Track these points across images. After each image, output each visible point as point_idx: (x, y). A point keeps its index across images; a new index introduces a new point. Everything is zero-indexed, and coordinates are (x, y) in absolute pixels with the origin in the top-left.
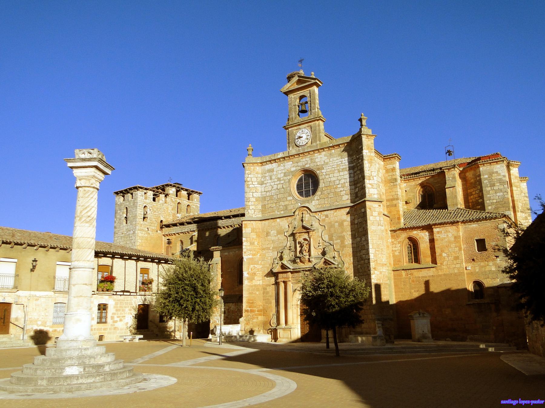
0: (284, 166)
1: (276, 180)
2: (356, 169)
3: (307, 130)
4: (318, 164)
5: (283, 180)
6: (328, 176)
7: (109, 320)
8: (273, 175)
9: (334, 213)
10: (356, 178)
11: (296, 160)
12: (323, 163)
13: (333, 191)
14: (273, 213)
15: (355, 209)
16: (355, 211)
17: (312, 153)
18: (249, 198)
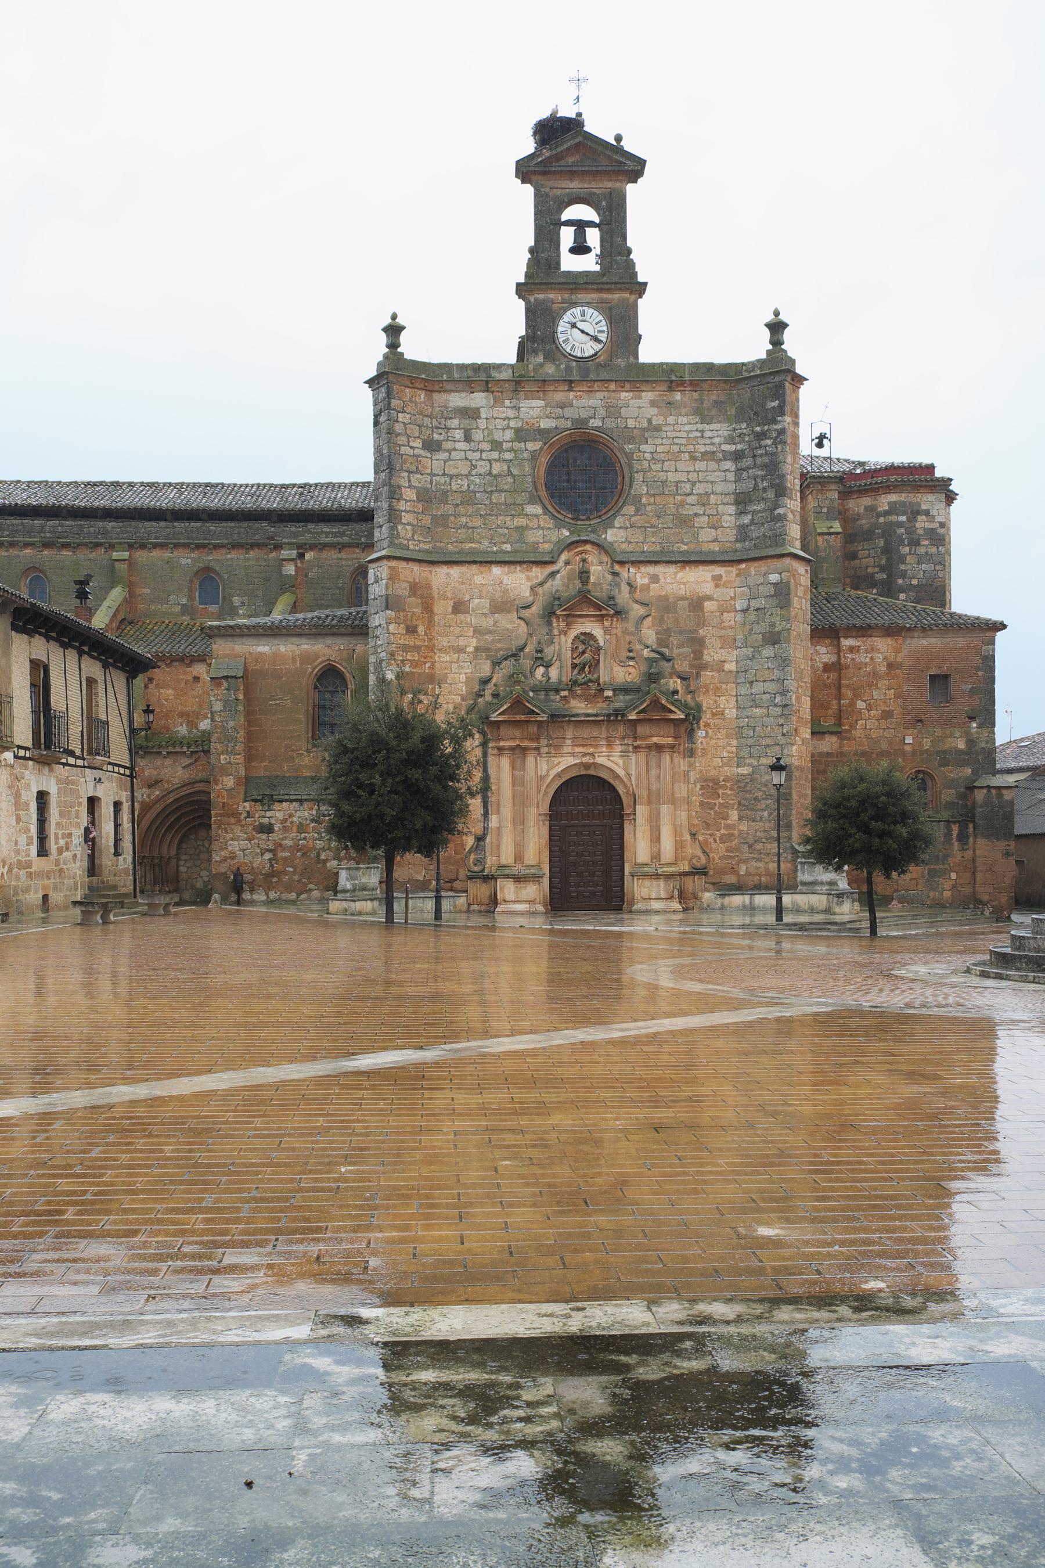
0: (517, 408)
1: (486, 446)
2: (749, 462)
3: (596, 313)
4: (631, 423)
5: (511, 450)
6: (659, 466)
7: (53, 848)
8: (477, 428)
9: (676, 574)
10: (747, 485)
11: (559, 397)
12: (645, 425)
13: (673, 510)
14: (473, 545)
15: (739, 570)
16: (737, 575)
17: (612, 386)
18: (400, 487)
